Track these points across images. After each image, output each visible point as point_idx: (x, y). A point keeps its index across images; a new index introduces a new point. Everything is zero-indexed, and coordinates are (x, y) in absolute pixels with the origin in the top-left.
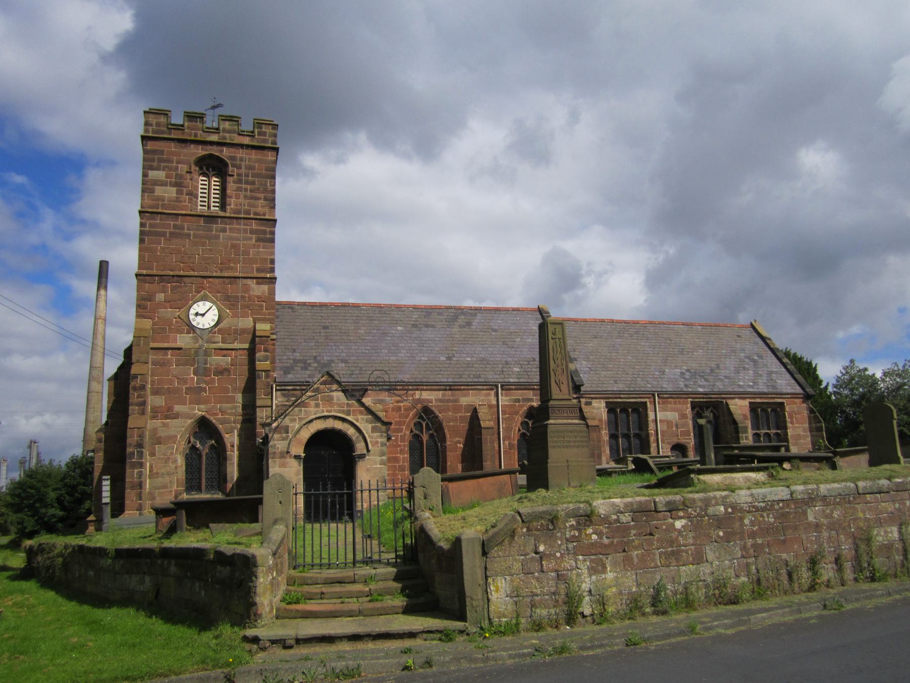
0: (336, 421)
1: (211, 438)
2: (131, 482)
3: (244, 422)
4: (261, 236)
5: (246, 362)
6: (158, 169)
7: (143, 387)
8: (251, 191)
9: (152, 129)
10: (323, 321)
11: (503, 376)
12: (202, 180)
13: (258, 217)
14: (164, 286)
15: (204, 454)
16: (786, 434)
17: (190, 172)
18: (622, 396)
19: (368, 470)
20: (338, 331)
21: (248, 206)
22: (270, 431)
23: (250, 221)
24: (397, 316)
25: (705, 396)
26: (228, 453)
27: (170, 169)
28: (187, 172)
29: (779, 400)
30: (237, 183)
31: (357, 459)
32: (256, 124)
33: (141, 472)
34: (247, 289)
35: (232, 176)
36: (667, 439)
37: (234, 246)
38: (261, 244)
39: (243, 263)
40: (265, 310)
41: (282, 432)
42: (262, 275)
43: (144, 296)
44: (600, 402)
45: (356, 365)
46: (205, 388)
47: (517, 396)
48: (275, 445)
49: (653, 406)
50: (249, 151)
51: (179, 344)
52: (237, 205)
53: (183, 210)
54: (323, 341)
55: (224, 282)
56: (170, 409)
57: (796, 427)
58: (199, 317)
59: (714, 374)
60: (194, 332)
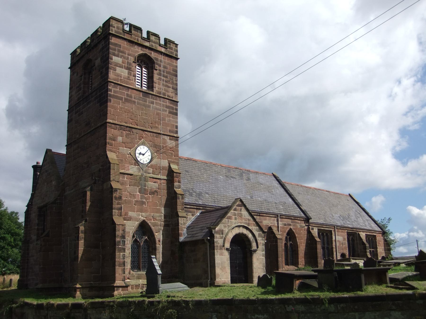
0: (244, 229)
1: (144, 234)
2: (118, 261)
3: (166, 225)
4: (171, 110)
5: (166, 188)
6: (118, 56)
7: (120, 198)
8: (166, 82)
9: (115, 30)
10: (184, 167)
11: (278, 210)
12: (137, 69)
13: (169, 98)
14: (122, 132)
15: (142, 244)
16: (377, 251)
17: (135, 63)
18: (324, 226)
19: (258, 259)
20: (193, 174)
21: (164, 90)
22: (215, 232)
23: (165, 100)
24: (216, 169)
25: (352, 229)
26: (157, 245)
27: (124, 58)
28: (133, 62)
29: (375, 234)
30: (158, 75)
31: (253, 253)
32: (168, 42)
33: (124, 255)
34: (165, 142)
35: (157, 70)
36: (339, 251)
37: (158, 114)
38: (171, 115)
39: (162, 126)
40: (173, 157)
41: (220, 234)
42: (172, 134)
43: (111, 137)
44: (316, 229)
45: (213, 196)
46: (145, 202)
47: (285, 222)
48: (217, 241)
49: (334, 232)
50: (165, 57)
51: (130, 172)
52: (159, 89)
53: (131, 85)
54: (190, 179)
55: (153, 135)
56: (126, 214)
57: (380, 248)
58: (141, 155)
59: (350, 219)
60: (139, 165)
